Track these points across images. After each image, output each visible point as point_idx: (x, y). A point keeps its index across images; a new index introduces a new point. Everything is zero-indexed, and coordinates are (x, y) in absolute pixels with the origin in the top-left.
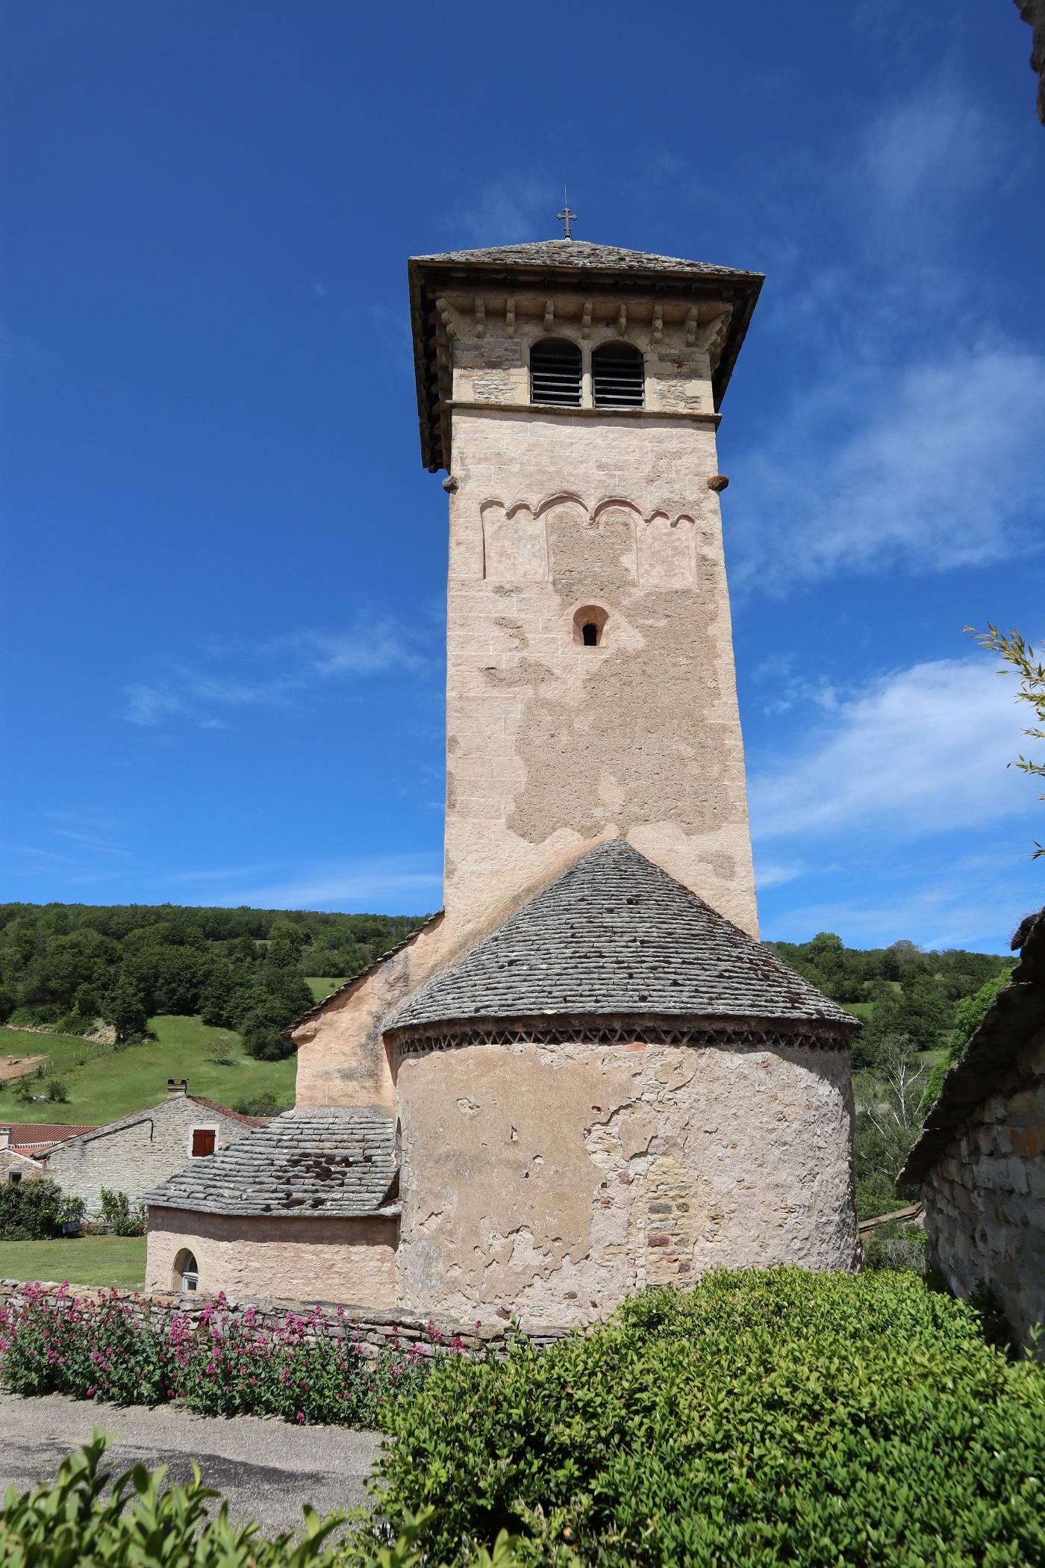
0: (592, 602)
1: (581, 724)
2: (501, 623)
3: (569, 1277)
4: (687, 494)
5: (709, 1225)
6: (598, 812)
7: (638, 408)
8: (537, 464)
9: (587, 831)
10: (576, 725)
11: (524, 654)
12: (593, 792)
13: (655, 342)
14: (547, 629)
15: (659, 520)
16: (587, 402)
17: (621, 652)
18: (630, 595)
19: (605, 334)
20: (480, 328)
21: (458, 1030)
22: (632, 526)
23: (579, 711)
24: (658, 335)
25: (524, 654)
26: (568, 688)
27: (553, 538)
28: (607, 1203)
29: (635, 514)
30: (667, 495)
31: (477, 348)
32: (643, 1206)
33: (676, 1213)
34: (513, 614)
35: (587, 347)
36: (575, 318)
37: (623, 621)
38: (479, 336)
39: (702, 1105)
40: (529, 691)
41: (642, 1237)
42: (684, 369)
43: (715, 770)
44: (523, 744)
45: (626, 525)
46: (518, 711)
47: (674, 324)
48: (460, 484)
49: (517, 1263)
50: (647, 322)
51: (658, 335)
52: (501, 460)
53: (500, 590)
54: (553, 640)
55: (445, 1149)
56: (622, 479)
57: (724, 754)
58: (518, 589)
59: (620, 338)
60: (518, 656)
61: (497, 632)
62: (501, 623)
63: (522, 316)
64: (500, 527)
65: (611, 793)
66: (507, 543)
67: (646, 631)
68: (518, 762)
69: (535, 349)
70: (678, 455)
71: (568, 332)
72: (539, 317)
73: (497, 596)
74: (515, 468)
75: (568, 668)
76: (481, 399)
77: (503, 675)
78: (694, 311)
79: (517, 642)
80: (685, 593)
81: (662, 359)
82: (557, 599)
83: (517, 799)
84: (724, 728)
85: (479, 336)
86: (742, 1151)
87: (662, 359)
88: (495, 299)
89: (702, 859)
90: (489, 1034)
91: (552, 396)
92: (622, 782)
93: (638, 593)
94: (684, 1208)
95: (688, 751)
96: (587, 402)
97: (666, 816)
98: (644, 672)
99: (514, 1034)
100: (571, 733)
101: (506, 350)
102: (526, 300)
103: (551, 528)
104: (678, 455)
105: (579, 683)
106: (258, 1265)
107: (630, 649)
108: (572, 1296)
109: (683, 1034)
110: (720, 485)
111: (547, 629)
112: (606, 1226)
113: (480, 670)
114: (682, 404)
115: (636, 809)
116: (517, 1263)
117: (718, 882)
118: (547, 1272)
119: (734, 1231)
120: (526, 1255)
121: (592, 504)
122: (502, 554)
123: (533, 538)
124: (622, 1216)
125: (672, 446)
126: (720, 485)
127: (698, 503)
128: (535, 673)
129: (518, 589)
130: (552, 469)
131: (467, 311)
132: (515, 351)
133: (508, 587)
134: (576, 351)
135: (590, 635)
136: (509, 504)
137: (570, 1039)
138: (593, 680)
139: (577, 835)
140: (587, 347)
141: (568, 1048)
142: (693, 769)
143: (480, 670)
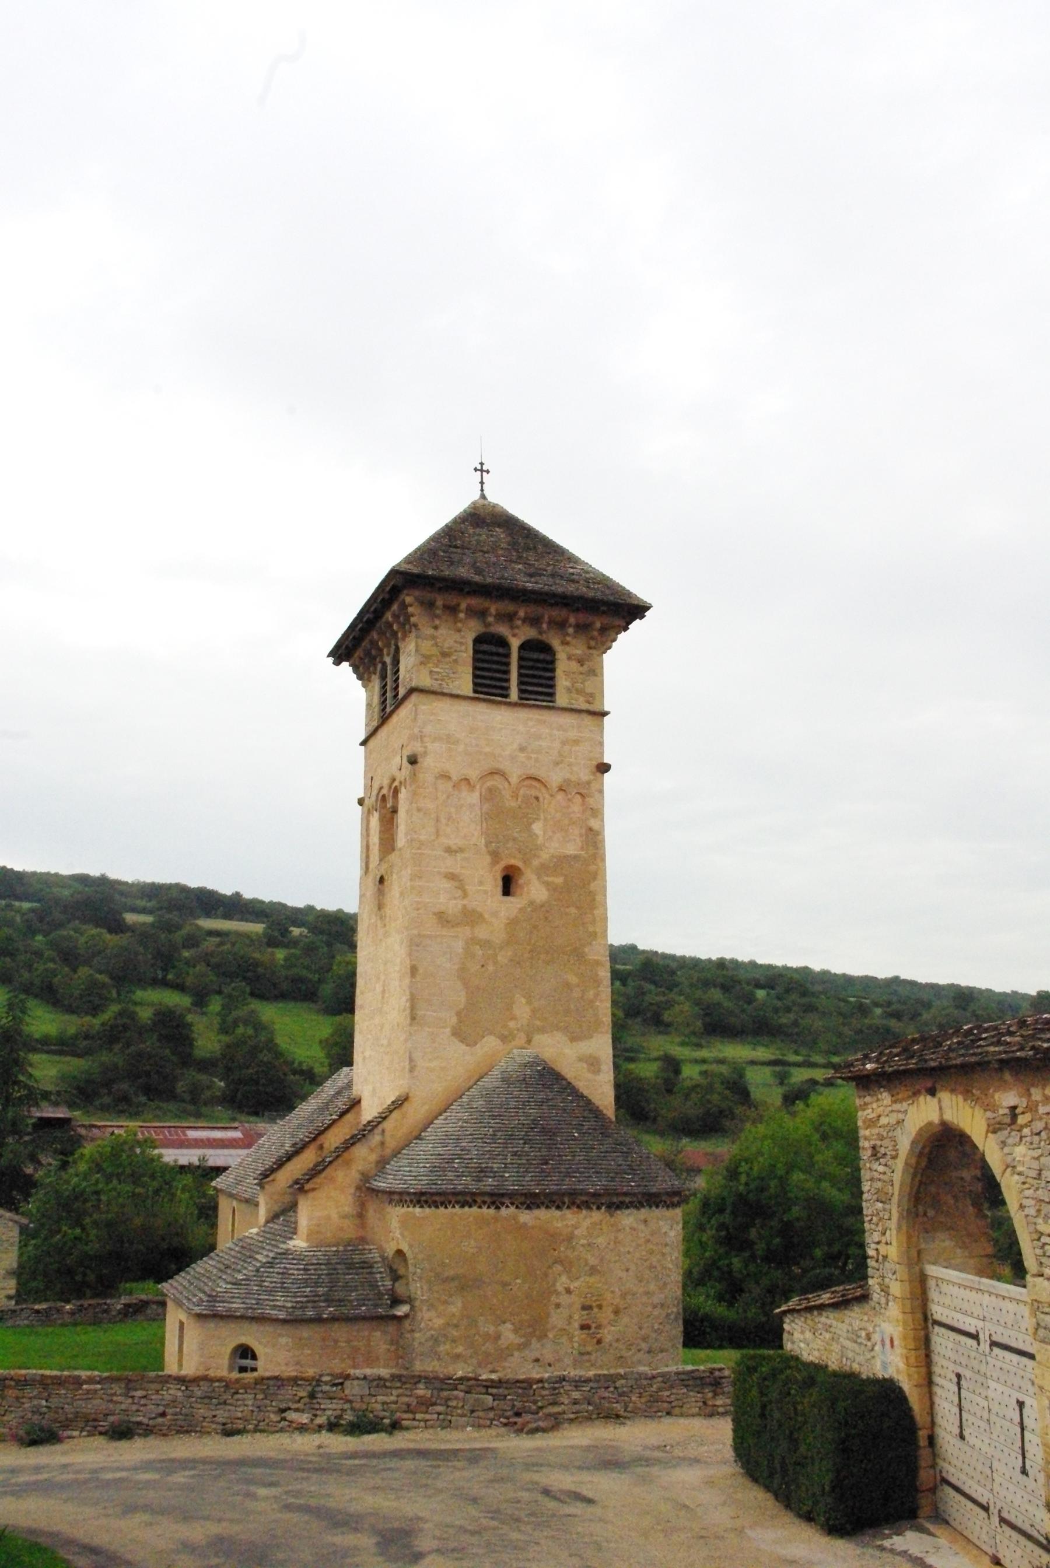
0: (513, 862)
1: (503, 958)
2: (452, 877)
3: (536, 1349)
4: (581, 775)
5: (612, 1316)
6: (512, 1024)
7: (551, 704)
8: (477, 745)
9: (504, 1039)
10: (499, 958)
11: (465, 902)
12: (509, 1007)
13: (565, 643)
14: (481, 883)
15: (560, 796)
16: (514, 695)
17: (531, 903)
18: (539, 857)
19: (528, 633)
20: (437, 622)
21: (460, 1198)
22: (541, 799)
23: (501, 948)
24: (568, 639)
25: (465, 902)
26: (494, 929)
27: (486, 806)
28: (558, 1306)
29: (544, 790)
30: (568, 776)
31: (434, 638)
32: (578, 1306)
33: (596, 1310)
34: (457, 870)
35: (515, 643)
36: (509, 618)
37: (533, 878)
38: (436, 628)
39: (611, 1246)
40: (467, 931)
41: (576, 1325)
42: (585, 669)
43: (591, 994)
44: (462, 974)
45: (537, 798)
46: (459, 946)
47: (582, 628)
48: (419, 760)
49: (503, 1343)
50: (561, 625)
51: (568, 639)
52: (450, 740)
53: (449, 850)
54: (486, 892)
55: (452, 1273)
56: (537, 760)
57: (597, 982)
58: (461, 850)
59: (540, 637)
60: (460, 903)
61: (447, 884)
62: (452, 877)
63: (471, 612)
64: (448, 797)
65: (522, 1010)
66: (453, 810)
67: (547, 884)
68: (459, 985)
69: (478, 641)
70: (576, 742)
71: (502, 630)
72: (482, 614)
73: (447, 855)
74: (461, 748)
75: (495, 914)
76: (435, 686)
77: (449, 919)
78: (598, 625)
79: (460, 893)
80: (576, 857)
81: (569, 658)
82: (488, 859)
83: (458, 1014)
84: (598, 963)
85: (436, 628)
86: (631, 1273)
87: (569, 658)
88: (452, 599)
89: (580, 1060)
90: (484, 1202)
91: (489, 684)
92: (529, 1003)
93: (545, 856)
94: (600, 1307)
95: (573, 979)
96: (514, 695)
97: (558, 1029)
98: (546, 918)
99: (503, 1204)
100: (495, 963)
101: (456, 642)
102: (475, 602)
103: (483, 799)
104: (576, 742)
105: (502, 926)
106: (309, 1352)
107: (538, 901)
108: (537, 1360)
109: (602, 1204)
110: (604, 768)
111: (481, 883)
112: (557, 1319)
113: (434, 914)
114: (581, 699)
115: (538, 1023)
116: (503, 1343)
117: (590, 1076)
118: (521, 1347)
119: (625, 1320)
120: (508, 1335)
121: (514, 780)
122: (449, 818)
123: (471, 806)
124: (565, 1312)
125: (572, 734)
126: (604, 768)
127: (589, 783)
128: (471, 917)
129: (461, 850)
130: (487, 750)
131: (430, 605)
132: (461, 643)
133: (454, 847)
134: (503, 643)
135: (508, 884)
136: (455, 778)
137: (538, 1207)
138: (513, 923)
139: (499, 1042)
140: (515, 643)
141: (536, 1212)
142: (576, 993)
143: (434, 914)
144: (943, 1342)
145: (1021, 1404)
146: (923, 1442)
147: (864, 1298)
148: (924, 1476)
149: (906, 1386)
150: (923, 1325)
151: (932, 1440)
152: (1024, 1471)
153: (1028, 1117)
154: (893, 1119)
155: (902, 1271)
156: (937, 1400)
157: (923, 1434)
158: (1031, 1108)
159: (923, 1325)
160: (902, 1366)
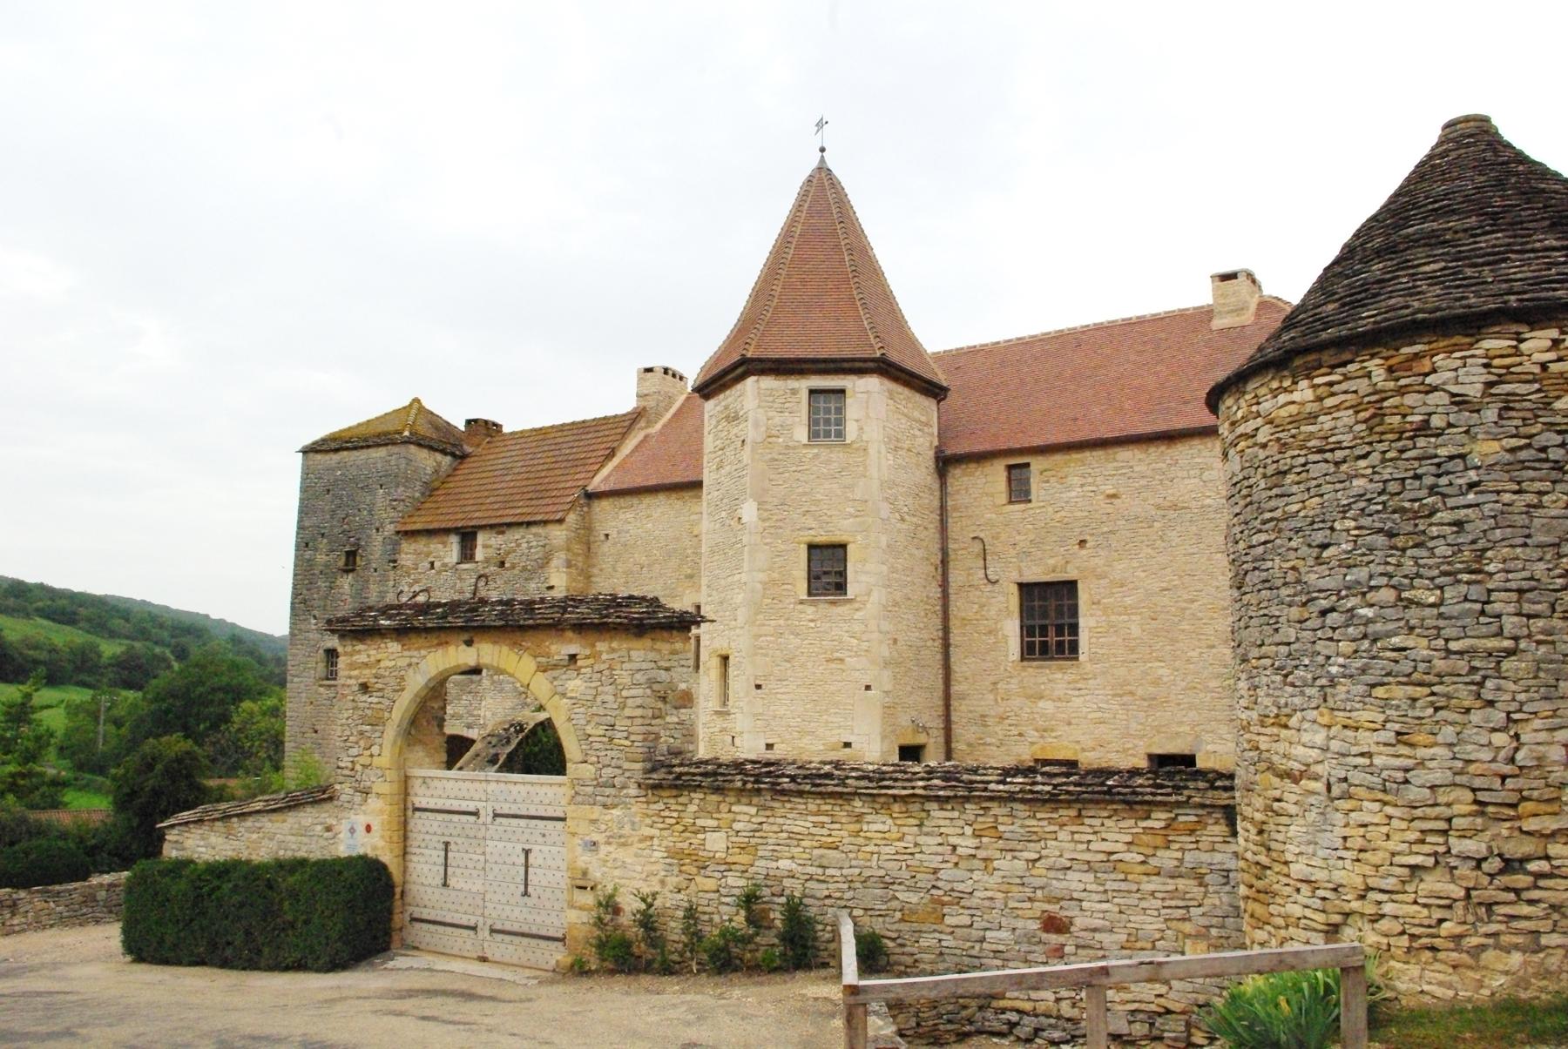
144: (419, 823)
145: (527, 852)
146: (398, 896)
147: (331, 799)
148: (397, 919)
149: (386, 858)
150: (405, 811)
151: (403, 892)
152: (526, 894)
153: (591, 661)
154: (402, 663)
155: (391, 775)
156: (411, 866)
157: (398, 890)
158: (596, 656)
159: (405, 811)
160: (381, 843)
